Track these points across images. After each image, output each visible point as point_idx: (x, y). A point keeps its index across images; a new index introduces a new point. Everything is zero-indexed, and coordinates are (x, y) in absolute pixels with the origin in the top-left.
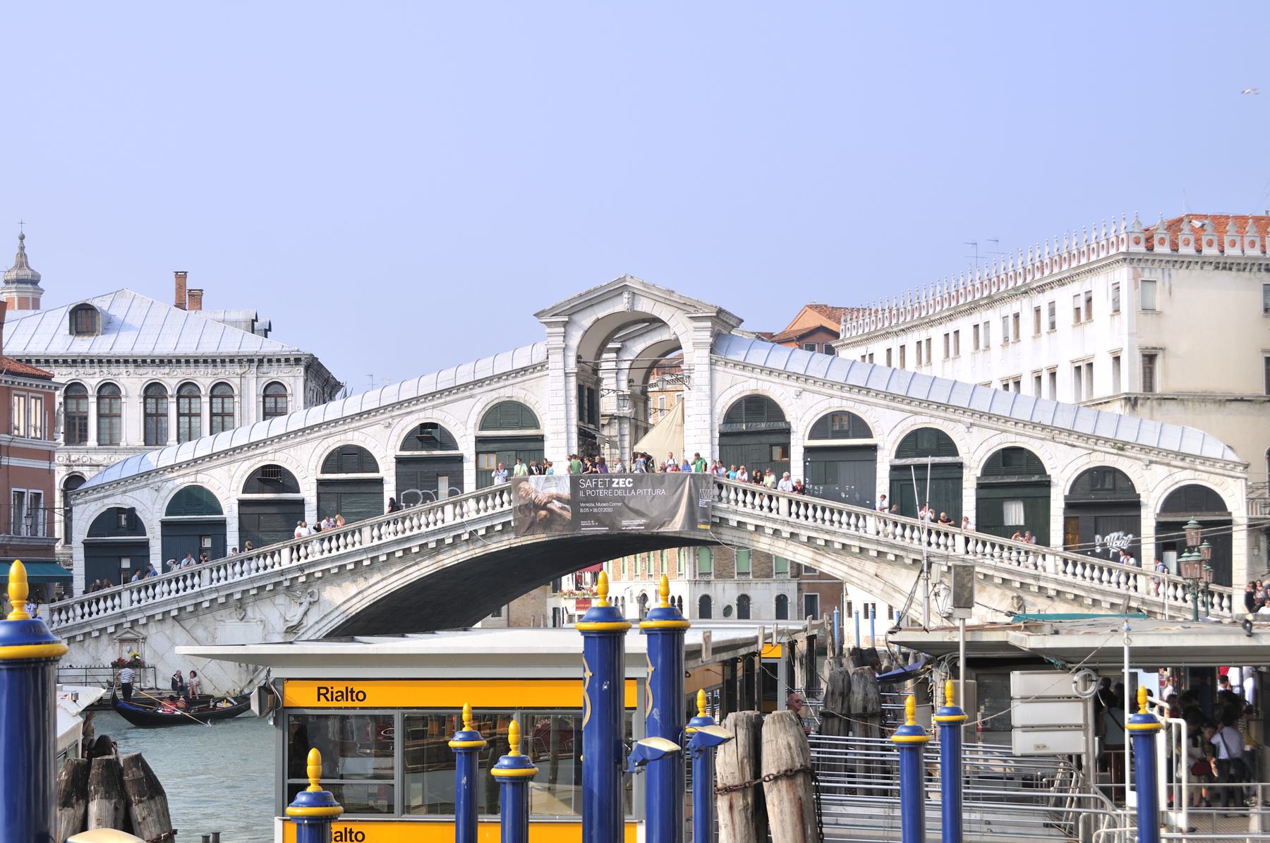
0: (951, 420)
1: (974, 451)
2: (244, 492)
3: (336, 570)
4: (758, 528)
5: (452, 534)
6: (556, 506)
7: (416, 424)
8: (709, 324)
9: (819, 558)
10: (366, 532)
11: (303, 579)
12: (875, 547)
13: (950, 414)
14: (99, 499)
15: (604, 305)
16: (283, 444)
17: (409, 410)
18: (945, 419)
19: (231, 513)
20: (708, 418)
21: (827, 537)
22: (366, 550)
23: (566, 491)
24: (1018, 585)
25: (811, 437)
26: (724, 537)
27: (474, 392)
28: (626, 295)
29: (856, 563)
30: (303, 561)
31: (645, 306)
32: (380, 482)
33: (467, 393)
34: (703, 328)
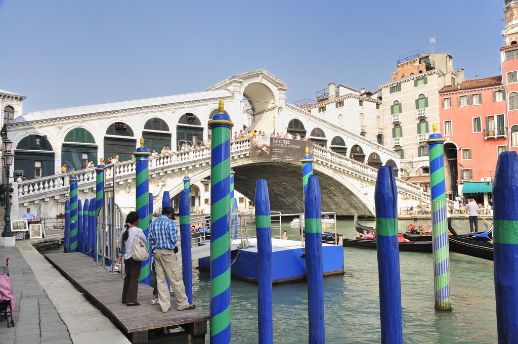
1: (349, 145)
2: (107, 133)
3: (177, 171)
4: (322, 162)
6: (264, 149)
7: (185, 113)
11: (161, 174)
12: (351, 171)
13: (344, 132)
14: (25, 129)
16: (126, 113)
17: (182, 106)
19: (100, 143)
21: (340, 167)
22: (192, 162)
23: (268, 143)
27: (207, 103)
28: (261, 76)
29: (343, 176)
30: (162, 166)
31: (265, 82)
32: (170, 135)
33: (205, 103)
34: (283, 94)
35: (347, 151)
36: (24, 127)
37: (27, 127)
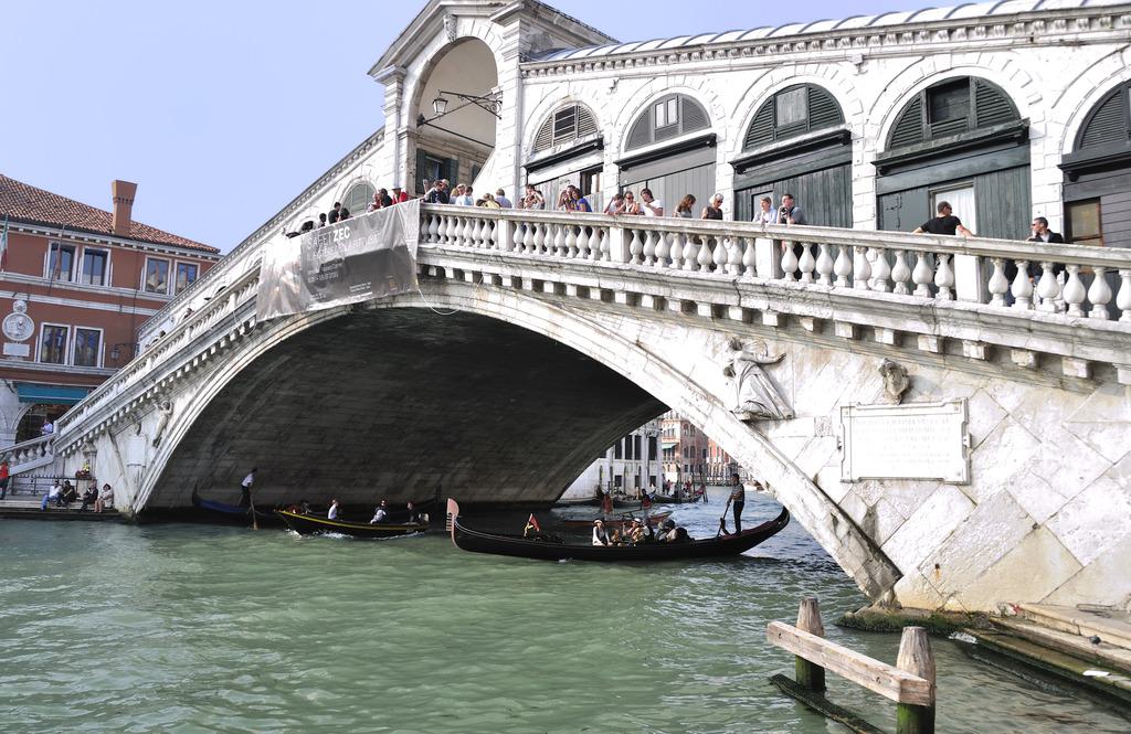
0: (830, 60)
4: (478, 276)
5: (233, 328)
8: (517, 24)
9: (557, 318)
10: (187, 331)
15: (432, 43)
17: (295, 213)
18: (819, 62)
20: (512, 151)
21: (555, 277)
24: (888, 338)
25: (629, 146)
26: (453, 300)
27: (337, 179)
28: (445, 21)
29: (608, 322)
31: (466, 28)
33: (331, 183)
35: (856, 147)
36: (150, 330)
37: (150, 330)
